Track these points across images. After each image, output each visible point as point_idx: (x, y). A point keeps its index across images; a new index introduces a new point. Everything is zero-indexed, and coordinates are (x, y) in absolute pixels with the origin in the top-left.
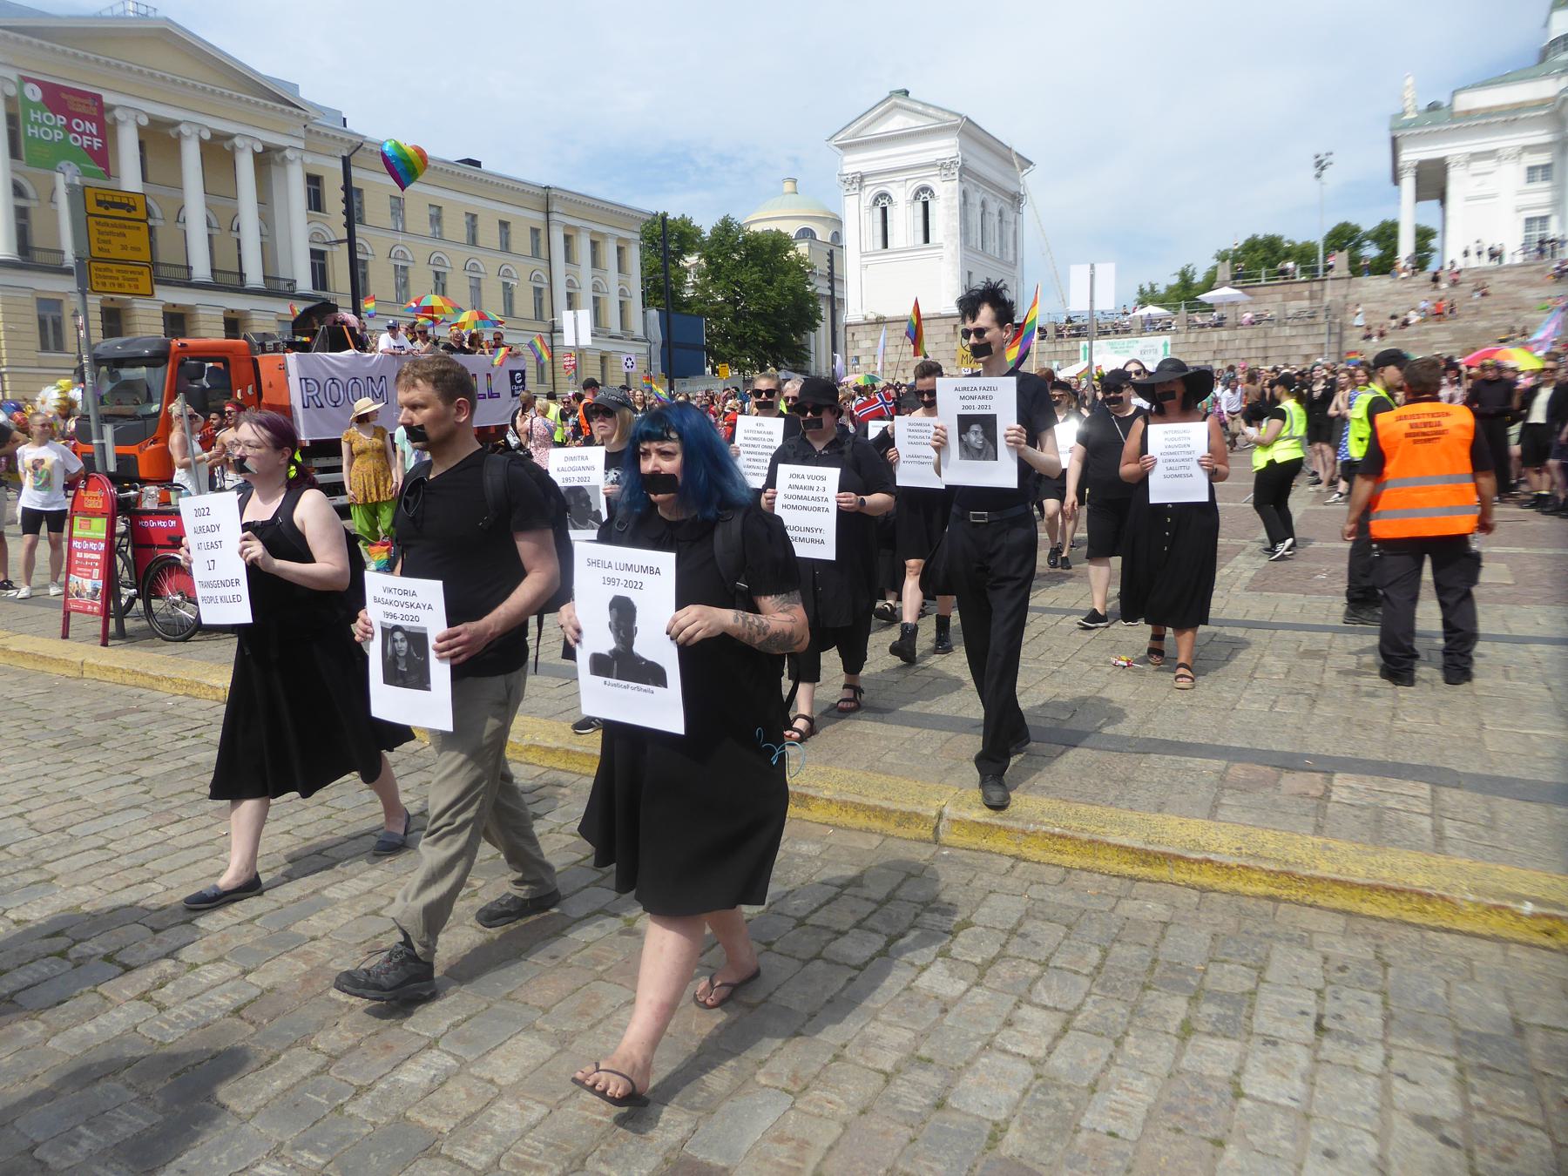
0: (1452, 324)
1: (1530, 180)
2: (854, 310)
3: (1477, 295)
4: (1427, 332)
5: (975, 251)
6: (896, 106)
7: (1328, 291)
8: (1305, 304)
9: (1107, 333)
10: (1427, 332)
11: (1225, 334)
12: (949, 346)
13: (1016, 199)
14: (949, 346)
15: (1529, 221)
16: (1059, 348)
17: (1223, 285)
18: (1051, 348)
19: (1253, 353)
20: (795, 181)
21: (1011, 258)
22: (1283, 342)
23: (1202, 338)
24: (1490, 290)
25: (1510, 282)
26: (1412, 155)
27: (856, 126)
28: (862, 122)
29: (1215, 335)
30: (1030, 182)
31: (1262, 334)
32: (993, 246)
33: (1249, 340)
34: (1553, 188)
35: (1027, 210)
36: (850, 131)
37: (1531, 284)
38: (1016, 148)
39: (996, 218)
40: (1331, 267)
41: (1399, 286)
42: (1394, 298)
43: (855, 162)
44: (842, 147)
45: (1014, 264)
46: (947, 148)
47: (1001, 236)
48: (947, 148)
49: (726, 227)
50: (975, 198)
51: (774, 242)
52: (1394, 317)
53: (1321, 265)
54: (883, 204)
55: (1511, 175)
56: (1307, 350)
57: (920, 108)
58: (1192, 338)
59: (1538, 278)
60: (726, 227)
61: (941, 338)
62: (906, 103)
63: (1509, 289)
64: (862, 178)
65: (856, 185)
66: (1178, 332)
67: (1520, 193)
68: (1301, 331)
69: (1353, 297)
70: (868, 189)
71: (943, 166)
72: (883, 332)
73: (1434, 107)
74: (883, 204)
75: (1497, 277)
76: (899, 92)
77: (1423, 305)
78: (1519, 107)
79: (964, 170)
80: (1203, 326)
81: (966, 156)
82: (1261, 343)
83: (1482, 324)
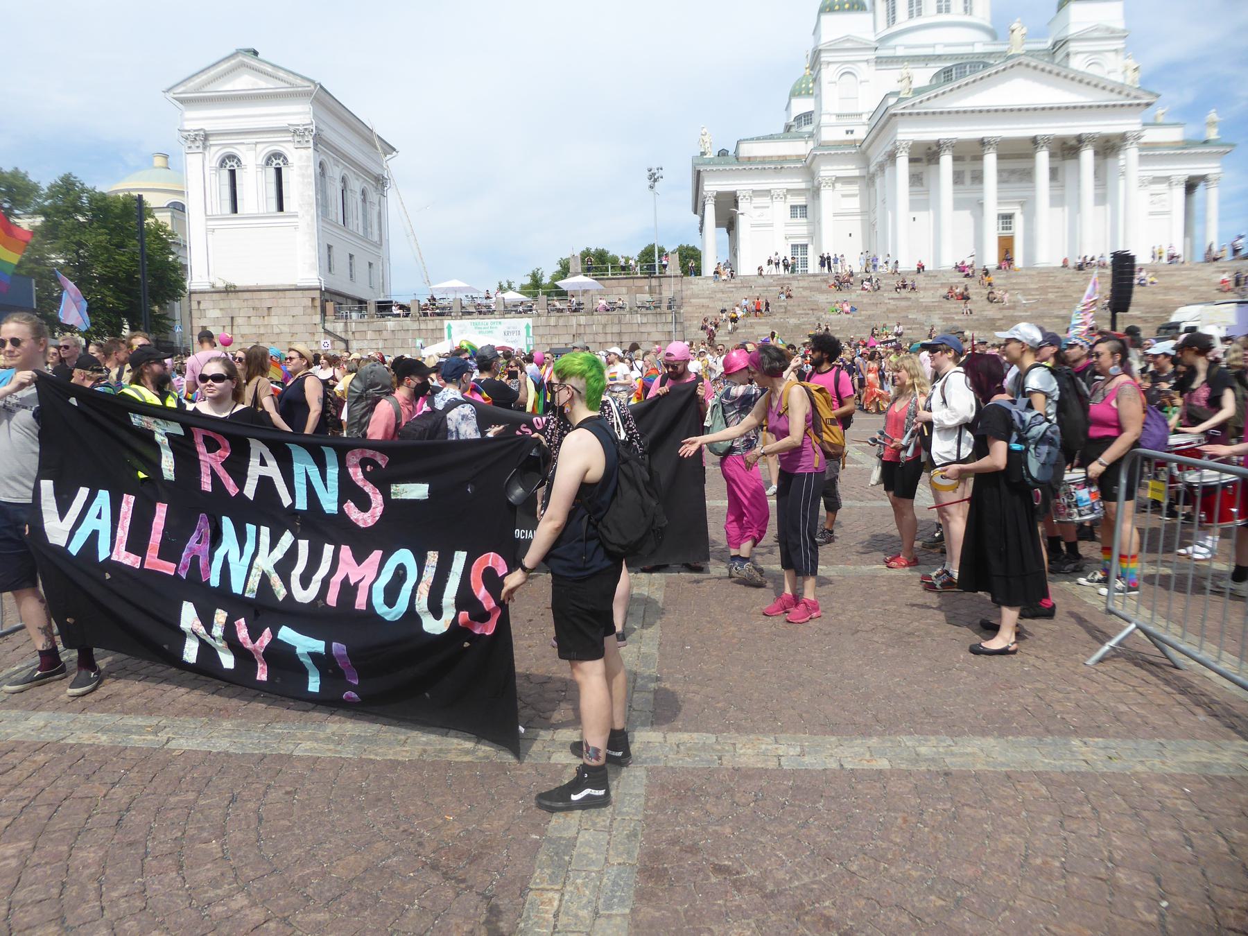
0: (770, 320)
1: (793, 215)
2: (198, 278)
3: (783, 297)
4: (752, 326)
5: (335, 225)
6: (243, 65)
7: (665, 287)
8: (647, 297)
9: (470, 313)
10: (752, 326)
11: (583, 319)
12: (307, 319)
13: (380, 182)
14: (307, 319)
15: (794, 247)
16: (423, 326)
17: (576, 274)
18: (415, 326)
19: (609, 338)
20: (166, 157)
21: (376, 238)
22: (635, 329)
23: (561, 322)
24: (792, 294)
25: (804, 288)
26: (711, 187)
27: (198, 80)
28: (204, 77)
29: (574, 320)
30: (394, 166)
32: (356, 223)
33: (605, 326)
34: (809, 224)
35: (391, 193)
36: (191, 84)
37: (822, 292)
38: (378, 131)
39: (359, 197)
40: (665, 266)
41: (721, 285)
42: (720, 295)
43: (199, 119)
44: (182, 101)
45: (379, 245)
46: (300, 114)
47: (365, 216)
48: (300, 114)
49: (67, 187)
50: (335, 172)
51: (125, 204)
52: (723, 311)
53: (657, 263)
54: (231, 167)
55: (780, 210)
56: (657, 337)
57: (269, 69)
58: (552, 321)
59: (824, 286)
60: (67, 187)
61: (299, 311)
62: (254, 63)
63: (805, 293)
64: (206, 137)
65: (199, 143)
66: (539, 315)
67: (787, 225)
68: (651, 319)
69: (687, 293)
70: (214, 149)
71: (296, 132)
72: (234, 303)
73: (723, 153)
74: (231, 167)
75: (795, 284)
76: (248, 51)
77: (744, 302)
78: (784, 159)
79: (319, 141)
80: (561, 311)
81: (322, 126)
82: (616, 329)
83: (793, 321)
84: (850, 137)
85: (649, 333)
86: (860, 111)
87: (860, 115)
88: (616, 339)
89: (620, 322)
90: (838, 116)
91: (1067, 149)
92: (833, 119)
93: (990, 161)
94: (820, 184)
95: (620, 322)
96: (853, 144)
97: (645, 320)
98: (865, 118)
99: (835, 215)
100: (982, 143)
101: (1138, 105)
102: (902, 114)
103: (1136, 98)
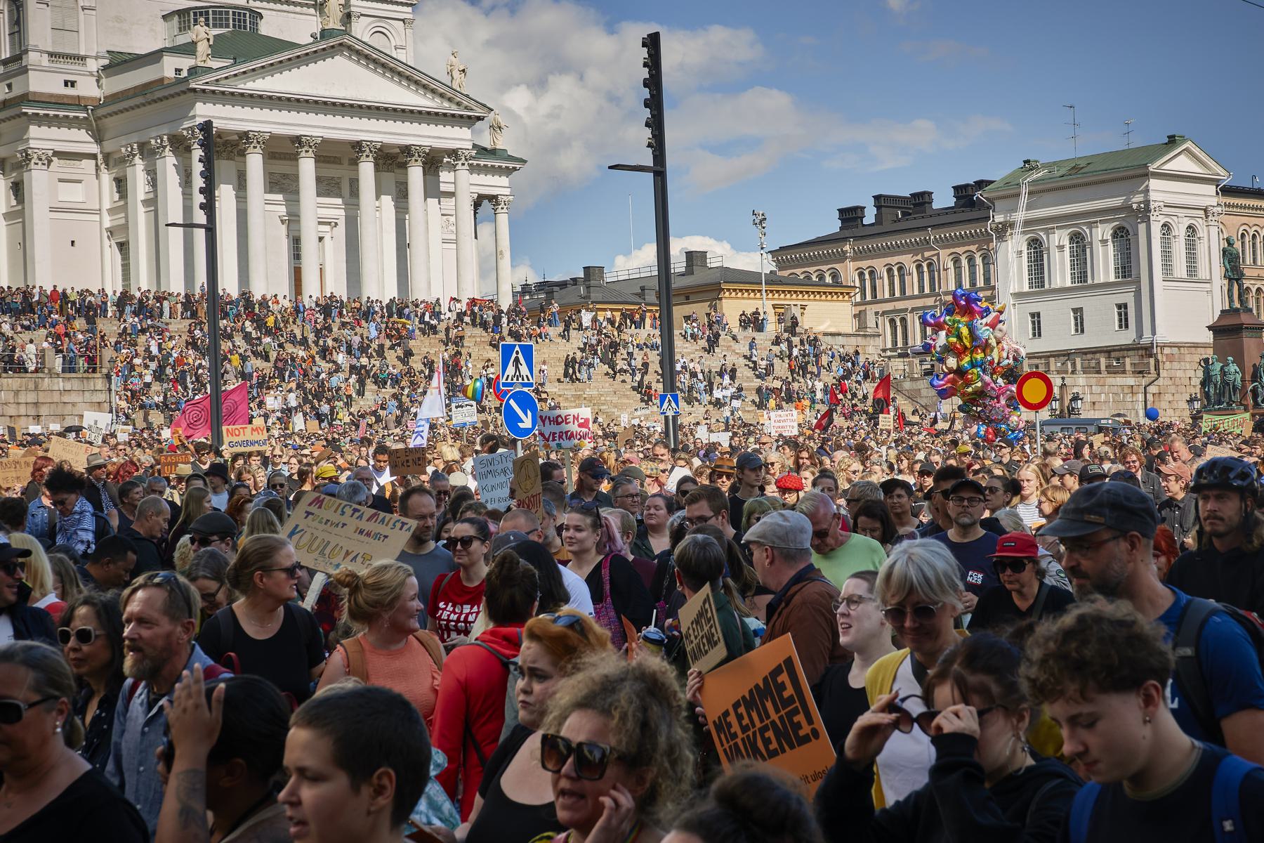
19: (23, 410)
31: (31, 386)
33: (17, 392)
82: (31, 397)
84: (70, 91)
85: (74, 404)
86: (82, 53)
87: (83, 58)
88: (32, 412)
89: (36, 387)
90: (51, 54)
91: (392, 160)
93: (307, 167)
94: (27, 158)
95: (36, 387)
96: (77, 103)
97: (68, 387)
98: (93, 65)
99: (53, 210)
100: (297, 140)
101: (469, 117)
102: (204, 91)
103: (466, 108)
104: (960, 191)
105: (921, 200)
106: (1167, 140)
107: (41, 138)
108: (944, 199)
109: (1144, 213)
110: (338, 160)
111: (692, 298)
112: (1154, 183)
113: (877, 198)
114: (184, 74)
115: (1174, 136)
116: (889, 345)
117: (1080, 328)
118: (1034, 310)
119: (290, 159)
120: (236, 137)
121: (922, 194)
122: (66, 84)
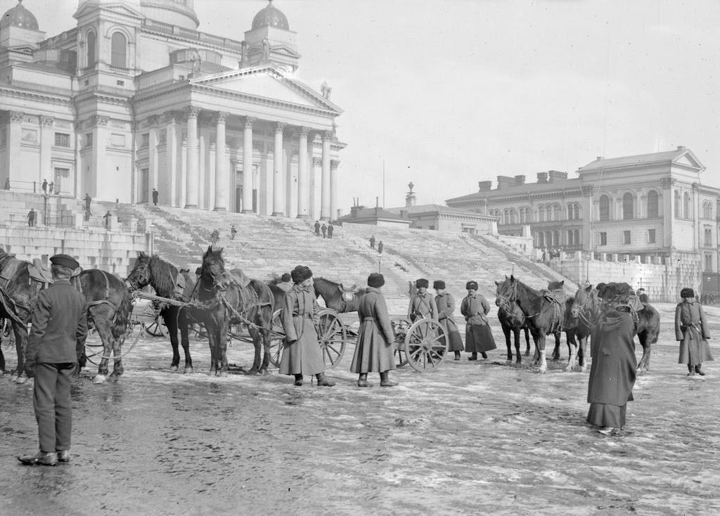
86: (127, 67)
87: (128, 70)
91: (292, 133)
92: (107, 69)
102: (196, 87)
104: (541, 176)
105: (520, 179)
106: (676, 149)
107: (103, 108)
108: (531, 179)
109: (668, 182)
110: (265, 129)
111: (422, 218)
112: (673, 170)
113: (499, 178)
114: (186, 78)
115: (681, 147)
116: (567, 244)
117: (628, 241)
118: (603, 231)
119: (240, 131)
120: (211, 115)
121: (521, 176)
122: (118, 84)
